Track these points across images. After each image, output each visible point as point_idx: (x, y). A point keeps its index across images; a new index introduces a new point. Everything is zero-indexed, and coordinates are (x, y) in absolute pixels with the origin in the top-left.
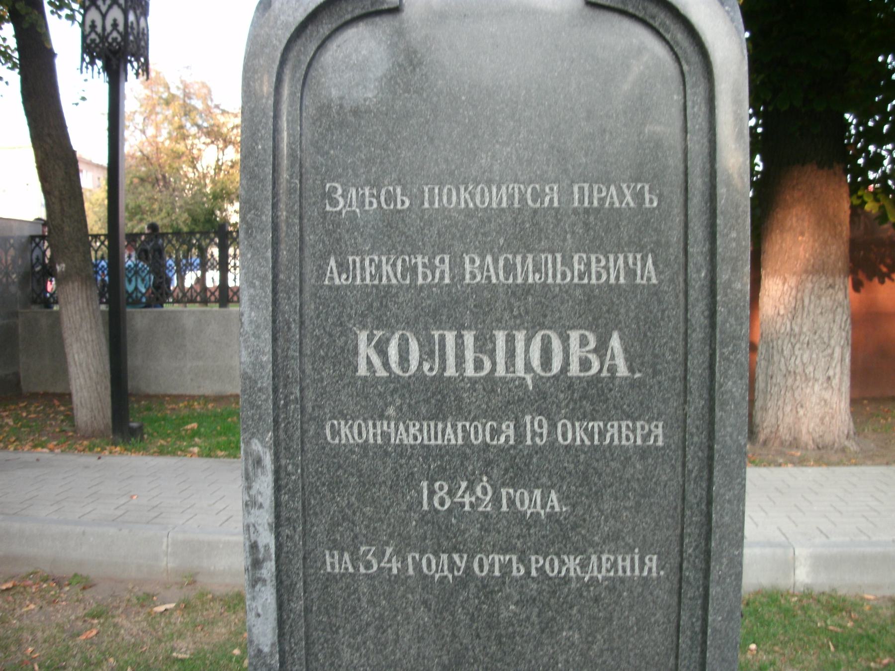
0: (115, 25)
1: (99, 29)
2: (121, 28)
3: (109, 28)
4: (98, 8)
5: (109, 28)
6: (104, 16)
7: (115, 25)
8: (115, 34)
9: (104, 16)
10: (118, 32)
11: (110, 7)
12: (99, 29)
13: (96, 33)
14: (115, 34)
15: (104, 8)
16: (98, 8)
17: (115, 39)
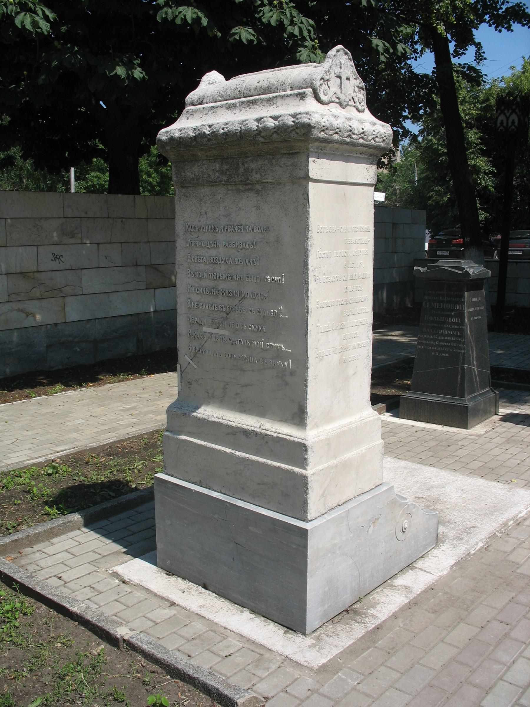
0: (513, 122)
1: (505, 125)
2: (516, 124)
3: (510, 124)
4: (505, 114)
5: (510, 124)
6: (508, 119)
7: (513, 122)
8: (513, 127)
9: (508, 119)
10: (515, 126)
11: (511, 114)
12: (505, 125)
13: (503, 126)
14: (513, 127)
15: (508, 114)
16: (505, 114)
17: (513, 130)
